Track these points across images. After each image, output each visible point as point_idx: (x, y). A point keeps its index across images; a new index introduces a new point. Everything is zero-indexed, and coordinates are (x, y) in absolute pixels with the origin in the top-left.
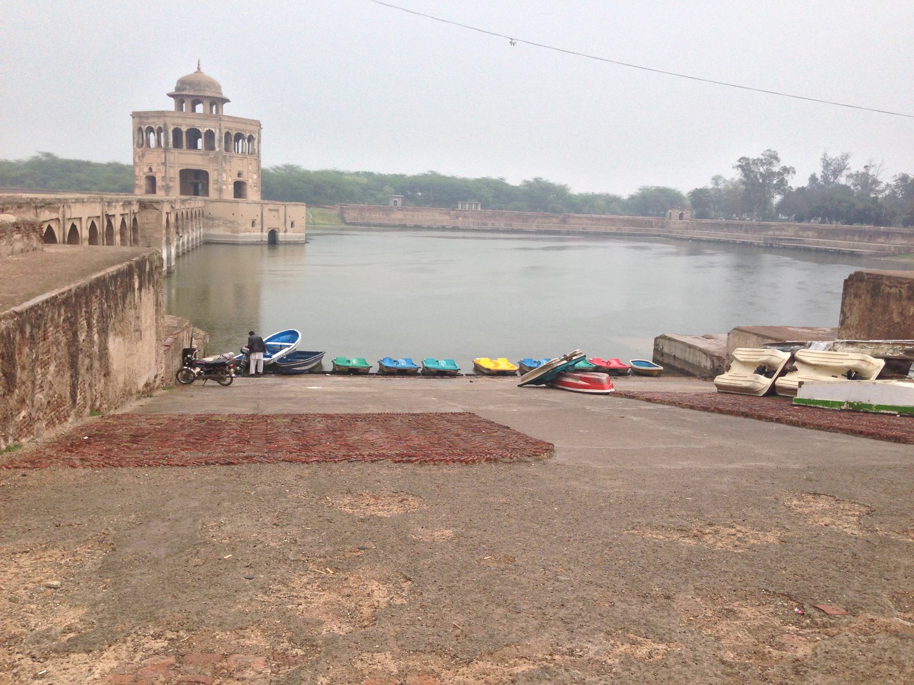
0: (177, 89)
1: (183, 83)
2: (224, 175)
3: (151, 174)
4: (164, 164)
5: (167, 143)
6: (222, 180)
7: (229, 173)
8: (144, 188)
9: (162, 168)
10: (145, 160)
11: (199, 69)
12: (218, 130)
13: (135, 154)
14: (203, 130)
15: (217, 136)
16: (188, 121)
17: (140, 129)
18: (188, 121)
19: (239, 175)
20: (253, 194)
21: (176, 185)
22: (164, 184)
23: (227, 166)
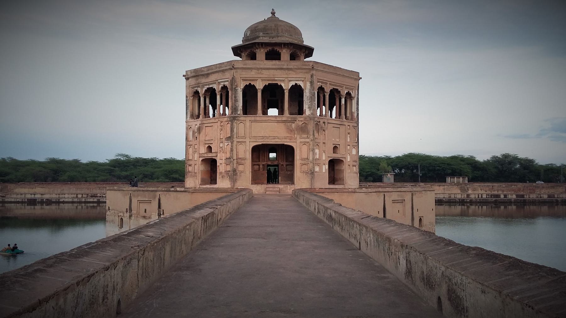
0: (245, 39)
1: (254, 29)
2: (317, 151)
3: (210, 155)
4: (229, 138)
5: (235, 110)
6: (310, 157)
7: (321, 145)
8: (199, 177)
9: (226, 145)
10: (202, 137)
11: (273, 13)
12: (308, 84)
13: (188, 128)
14: (286, 86)
15: (307, 94)
16: (266, 74)
17: (196, 93)
18: (266, 74)
19: (335, 148)
20: (351, 176)
21: (246, 169)
22: (229, 168)
23: (320, 138)
